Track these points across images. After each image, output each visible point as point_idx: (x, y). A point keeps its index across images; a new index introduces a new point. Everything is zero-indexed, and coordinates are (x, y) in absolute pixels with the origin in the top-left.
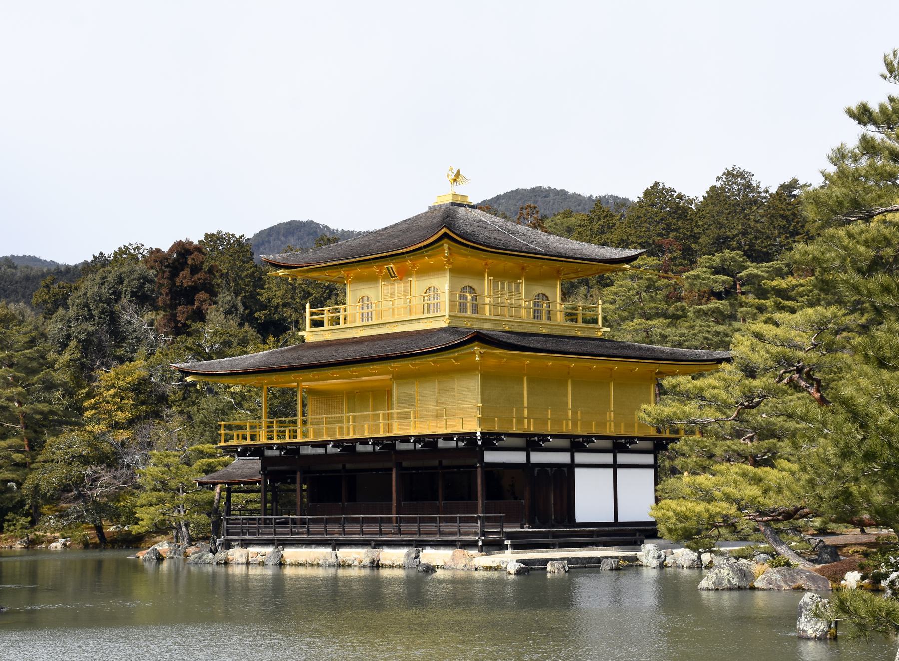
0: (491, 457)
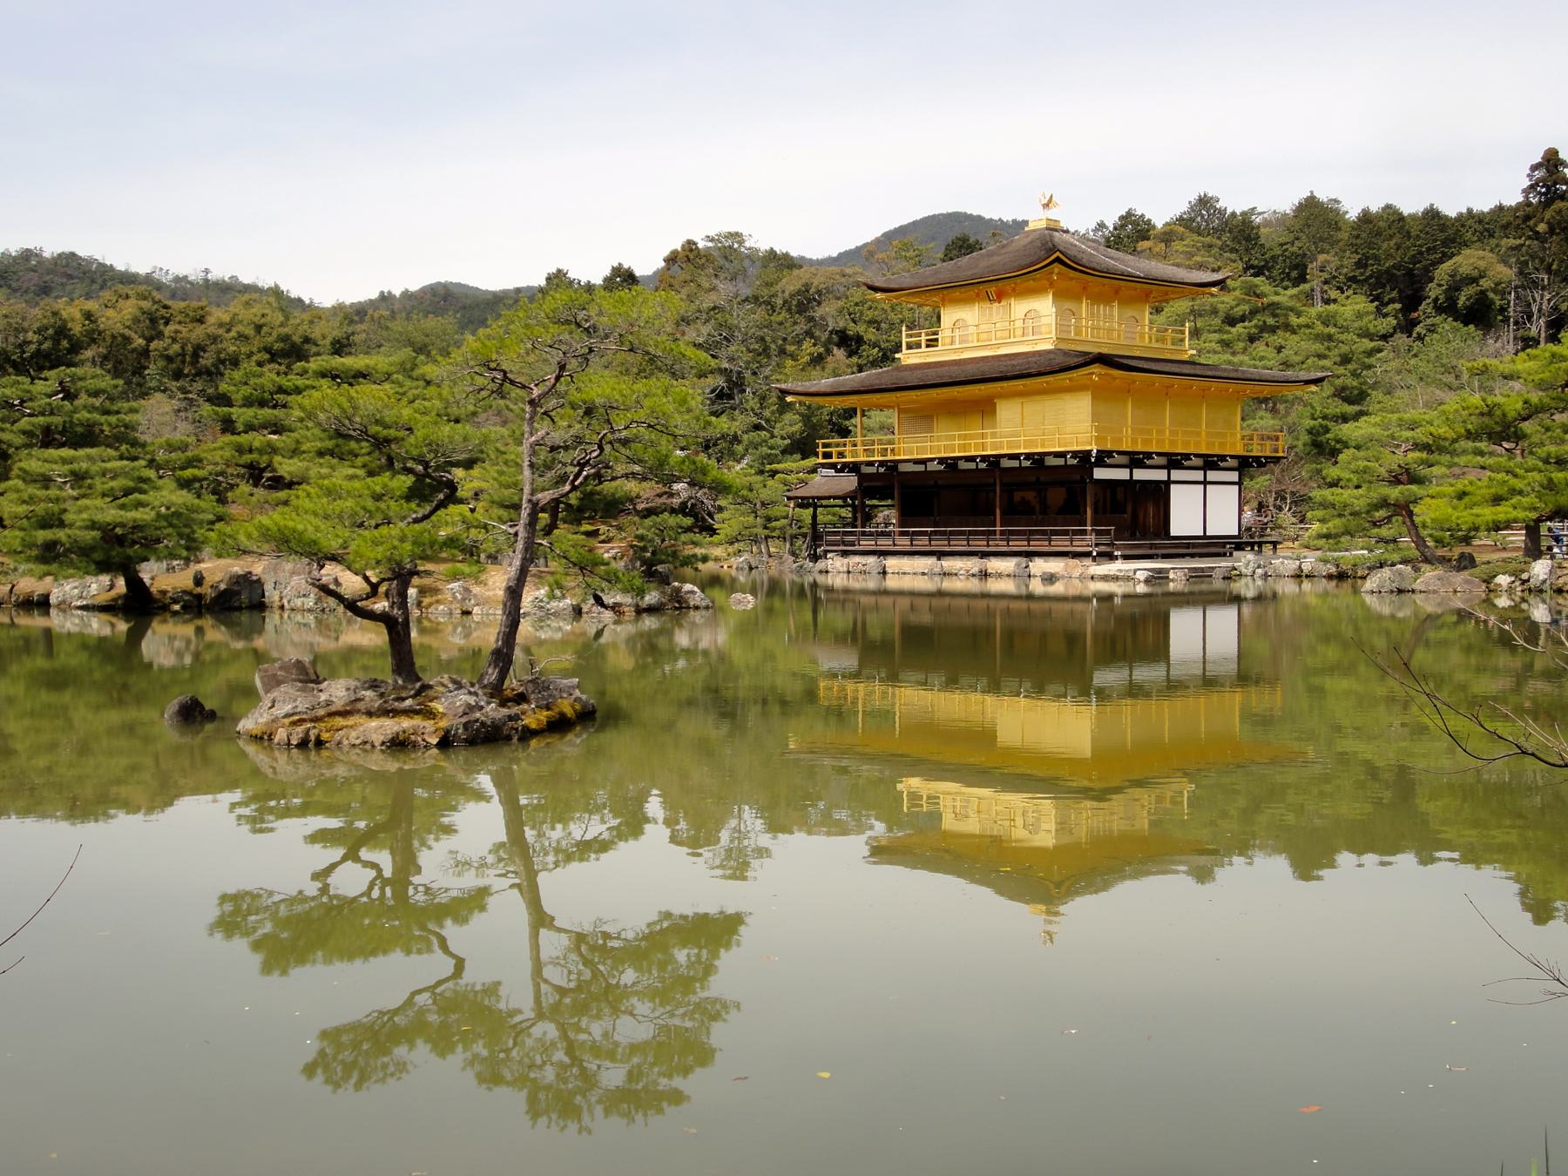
0: (1100, 474)
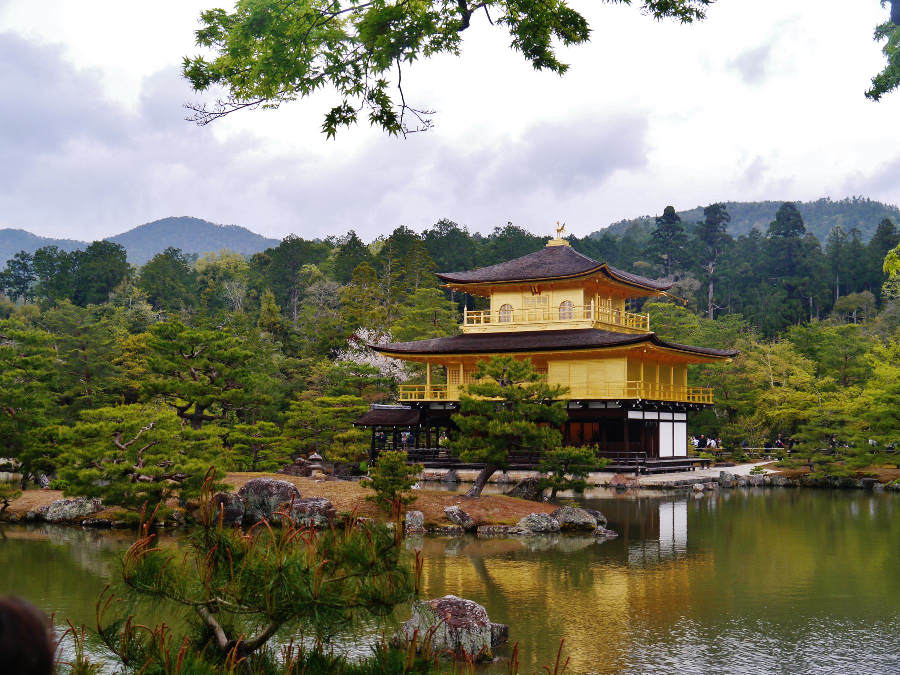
0: (633, 415)
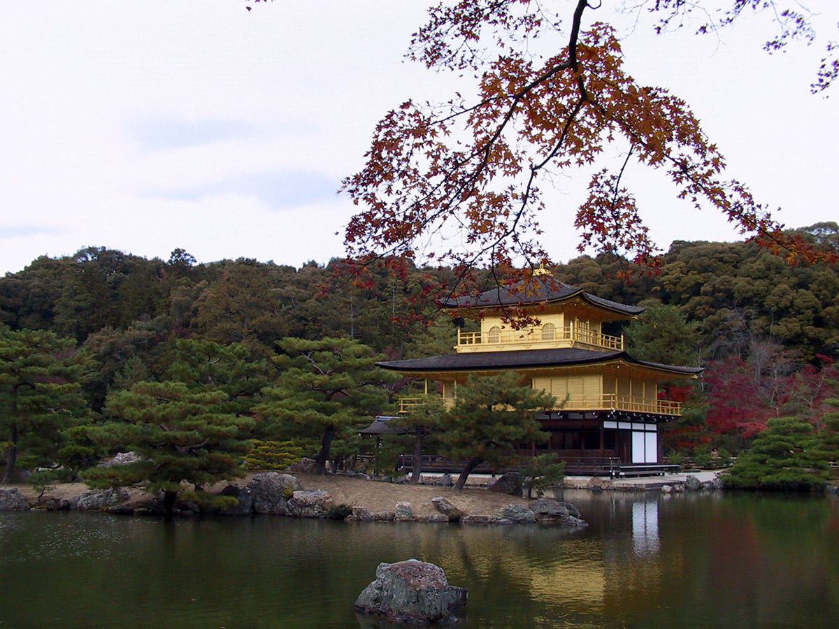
0: (607, 425)
